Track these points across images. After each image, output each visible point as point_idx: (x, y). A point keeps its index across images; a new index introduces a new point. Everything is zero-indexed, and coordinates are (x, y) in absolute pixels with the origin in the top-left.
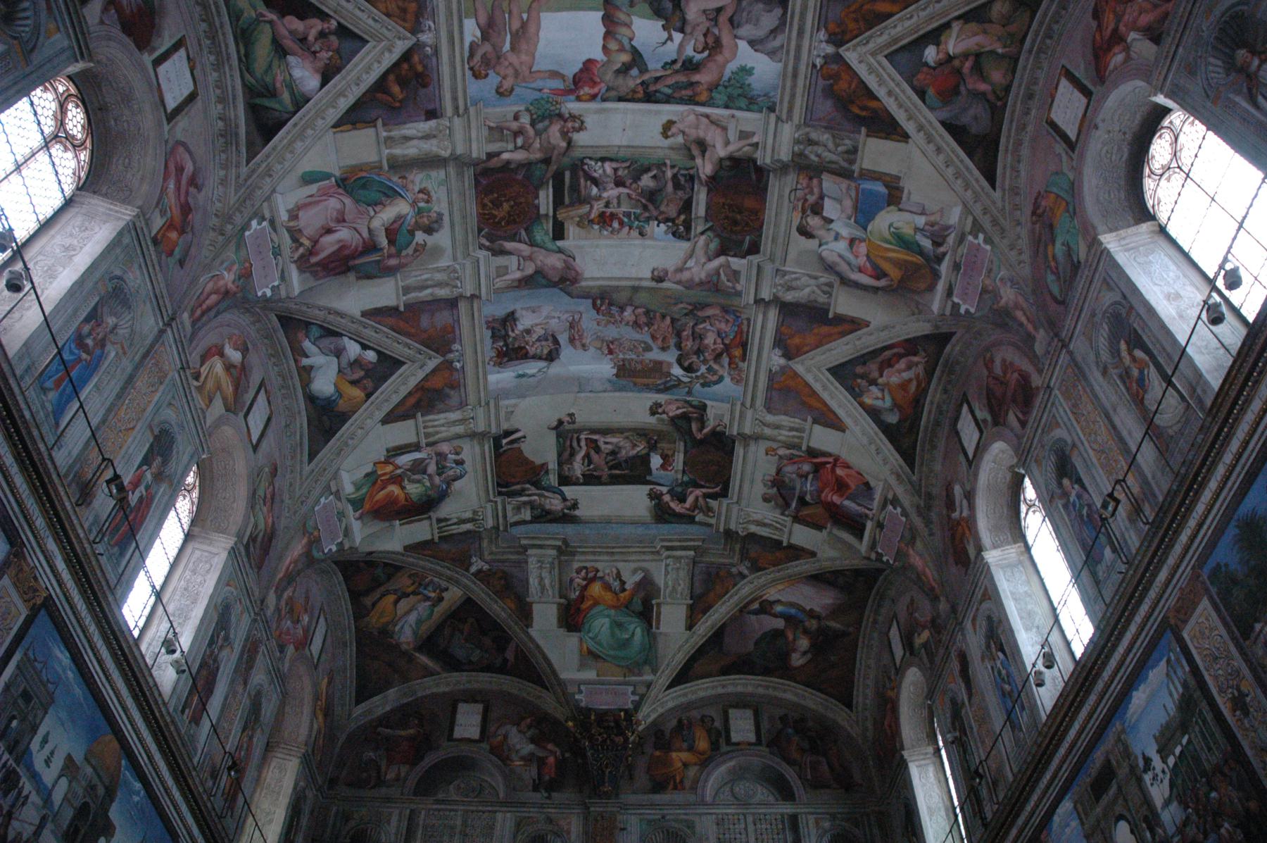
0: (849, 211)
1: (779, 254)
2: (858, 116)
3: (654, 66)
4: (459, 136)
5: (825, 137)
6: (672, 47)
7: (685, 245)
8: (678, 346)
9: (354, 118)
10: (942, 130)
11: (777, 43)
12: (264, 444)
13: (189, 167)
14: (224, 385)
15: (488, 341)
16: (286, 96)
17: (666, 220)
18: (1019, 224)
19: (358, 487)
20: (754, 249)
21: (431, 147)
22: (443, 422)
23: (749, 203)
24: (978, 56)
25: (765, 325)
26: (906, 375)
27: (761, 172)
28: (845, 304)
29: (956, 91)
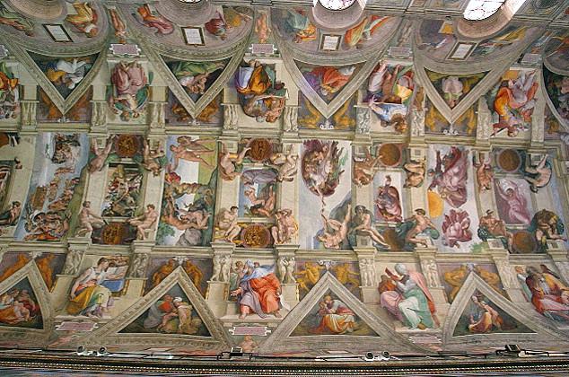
0: (110, 278)
1: (92, 251)
2: (152, 276)
3: (176, 201)
4: (158, 130)
5: (144, 265)
6: (184, 208)
7: (100, 215)
8: (49, 213)
9: (169, 93)
10: (146, 309)
11: (183, 243)
12: (44, 32)
13: (164, 31)
14: (80, 18)
15: (68, 134)
16: (180, 74)
17: (112, 207)
18: (102, 343)
19: (6, 68)
20: (94, 241)
21: (155, 120)
22: (33, 111)
23: (116, 239)
24: (178, 318)
25: (56, 248)
26: (19, 314)
27: (131, 241)
28: (62, 281)
29: (162, 313)
